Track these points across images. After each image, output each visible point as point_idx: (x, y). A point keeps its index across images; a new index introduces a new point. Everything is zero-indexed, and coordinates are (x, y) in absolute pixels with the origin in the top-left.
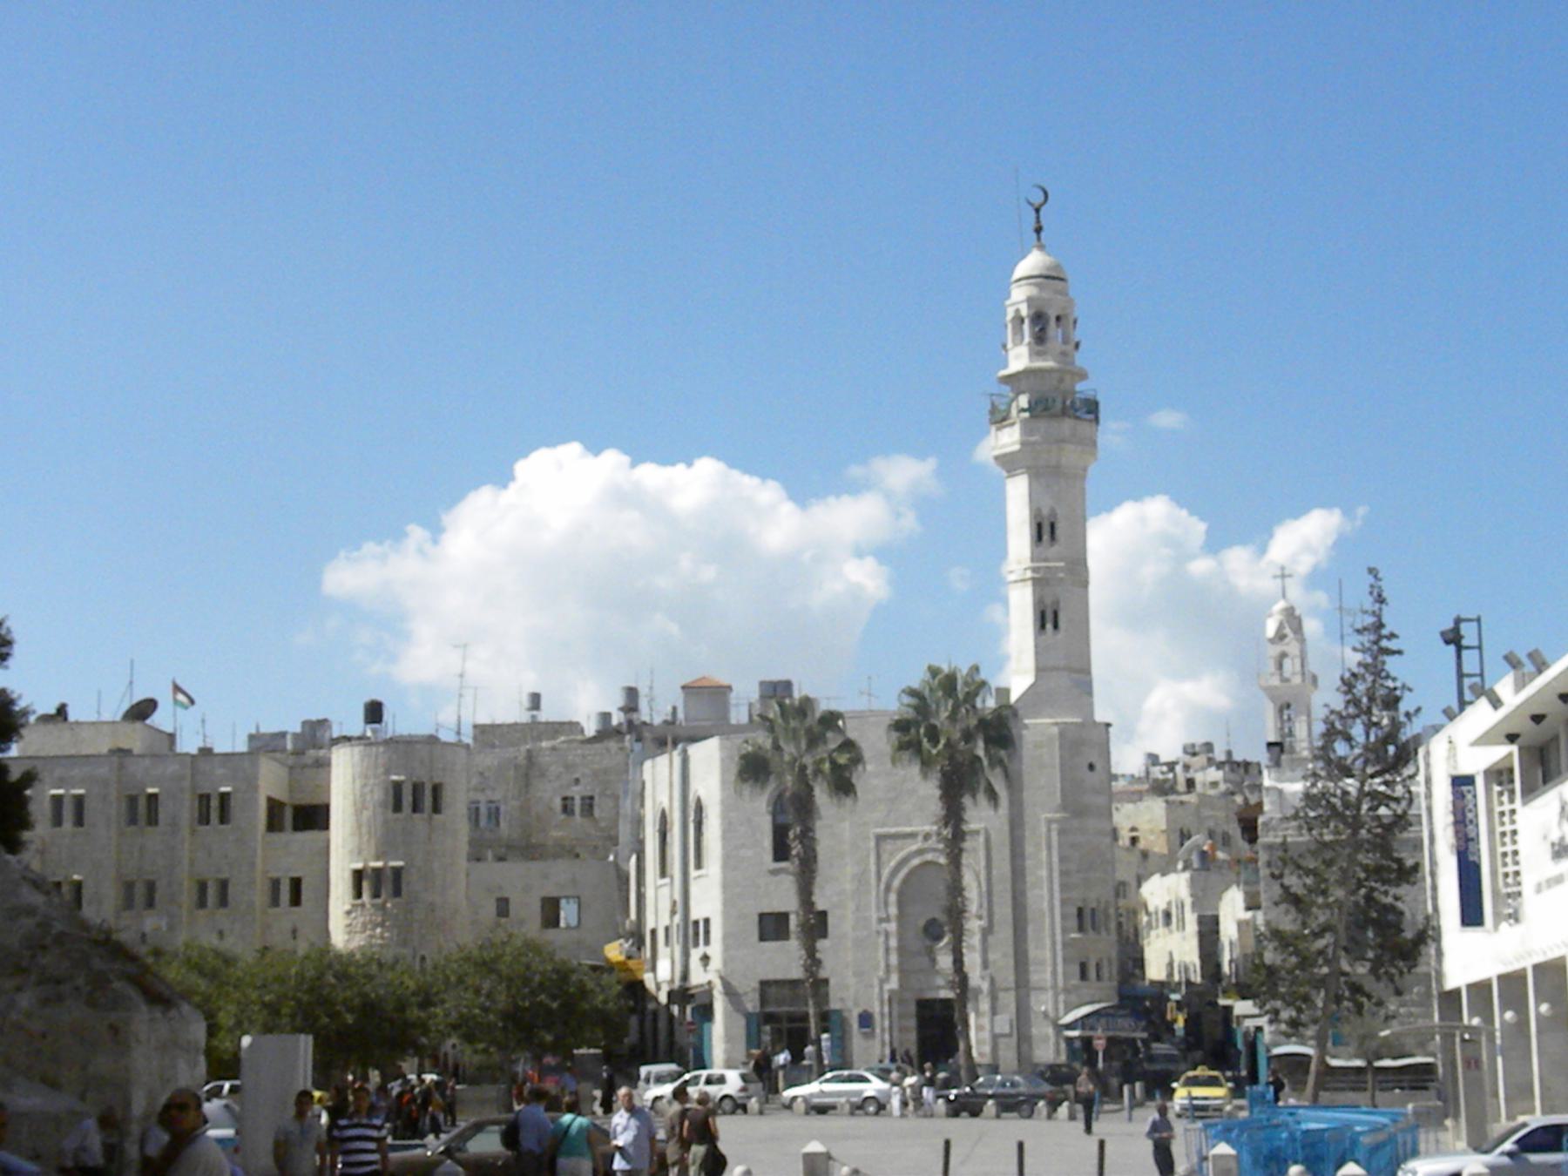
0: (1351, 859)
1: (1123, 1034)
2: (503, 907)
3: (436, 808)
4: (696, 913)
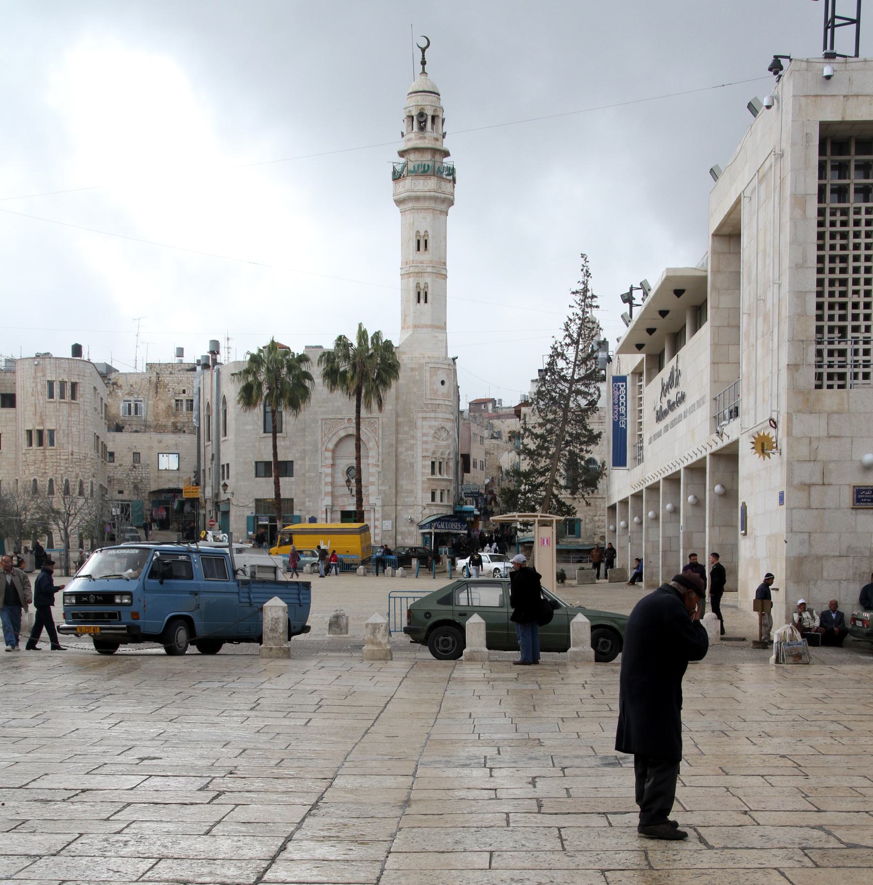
0: (562, 430)
1: (455, 531)
2: (136, 456)
3: (73, 397)
4: (223, 462)
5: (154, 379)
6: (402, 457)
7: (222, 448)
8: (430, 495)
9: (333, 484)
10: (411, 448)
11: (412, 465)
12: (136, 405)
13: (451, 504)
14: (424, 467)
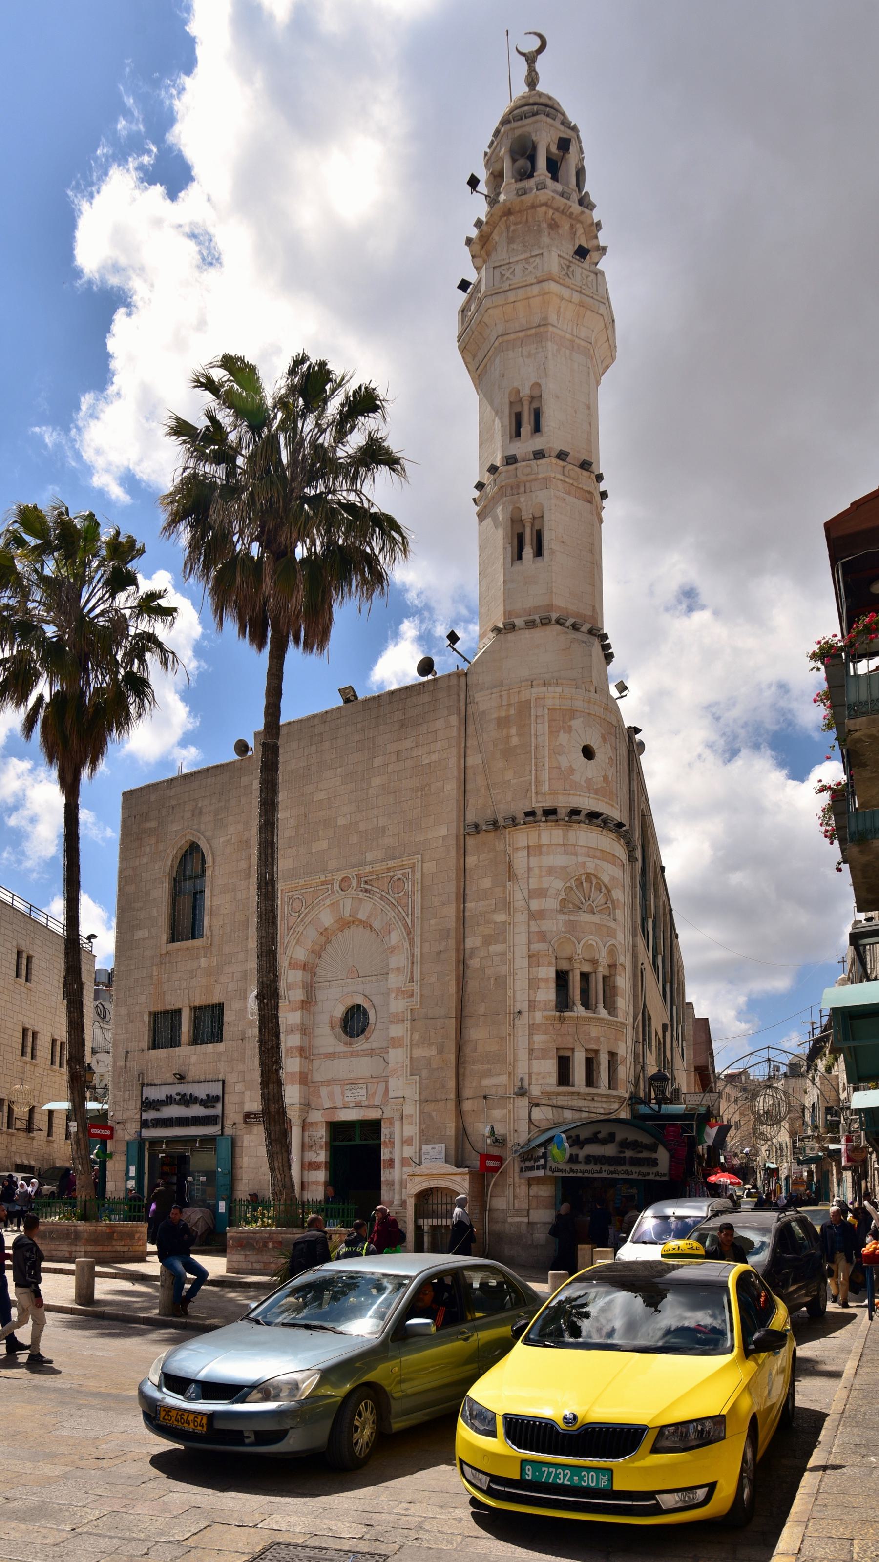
6: (475, 963)
8: (550, 1067)
10: (500, 934)
11: (501, 982)
14: (533, 984)
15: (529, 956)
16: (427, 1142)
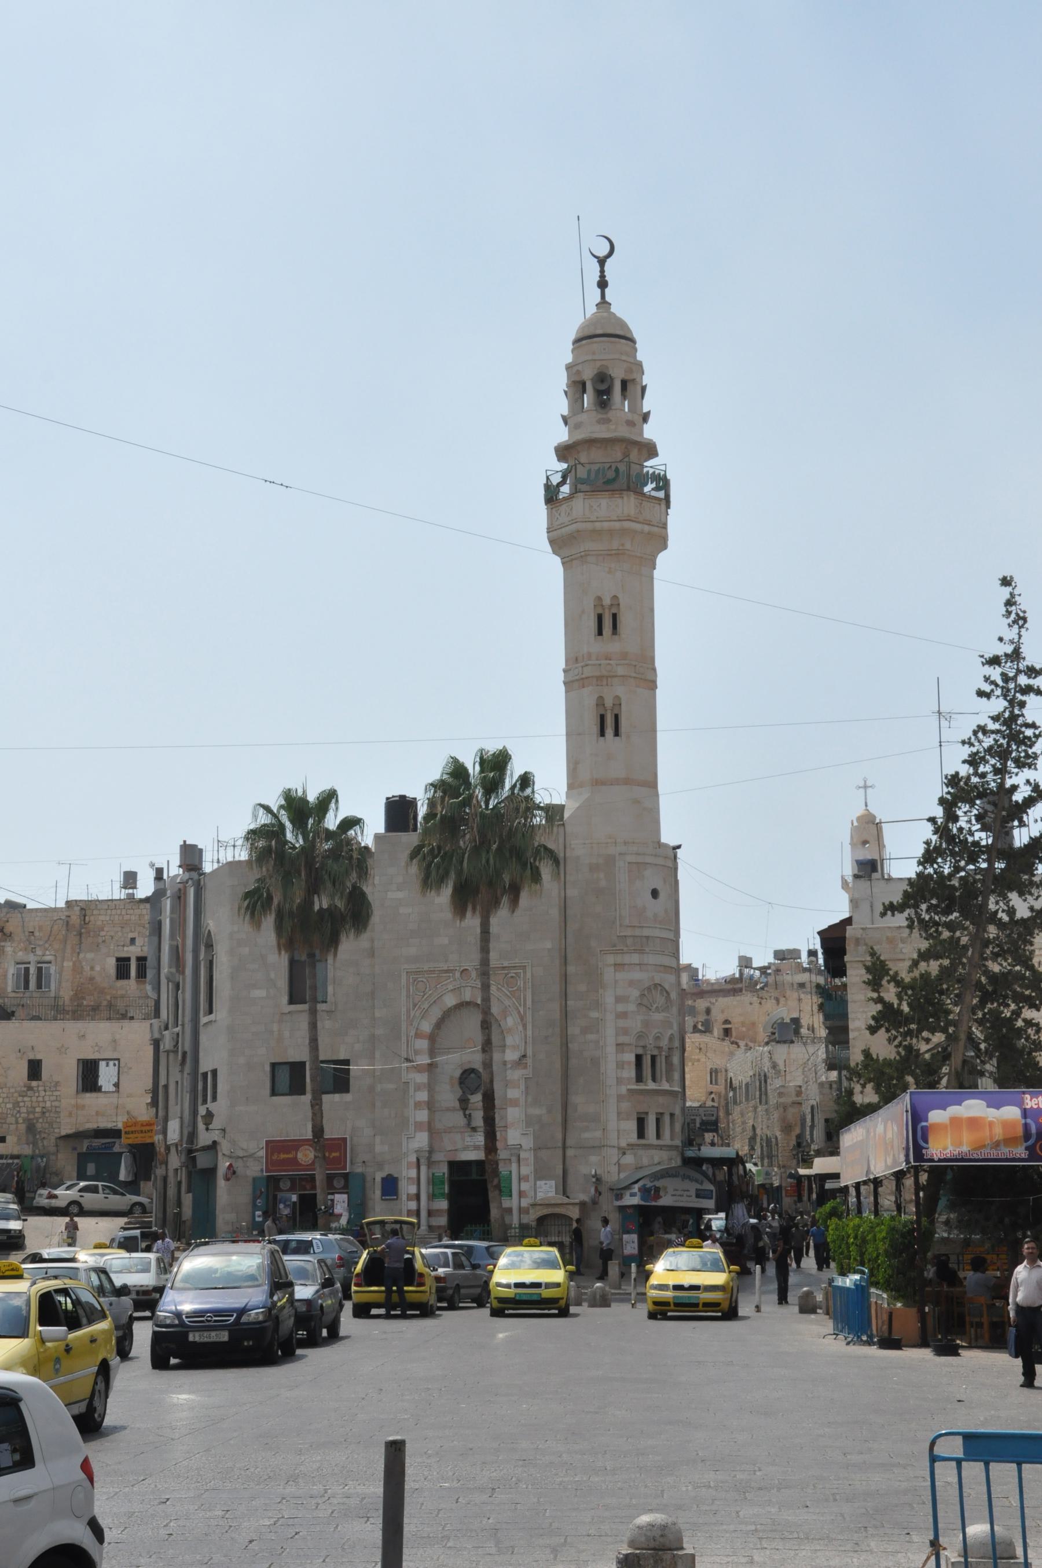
2: (35, 1069)
4: (205, 1066)
5: (75, 919)
6: (573, 1046)
7: (203, 1039)
8: (632, 1125)
9: (430, 1105)
11: (595, 1062)
12: (40, 970)
13: (678, 1142)
14: (620, 1065)
15: (617, 1045)
16: (541, 1178)
